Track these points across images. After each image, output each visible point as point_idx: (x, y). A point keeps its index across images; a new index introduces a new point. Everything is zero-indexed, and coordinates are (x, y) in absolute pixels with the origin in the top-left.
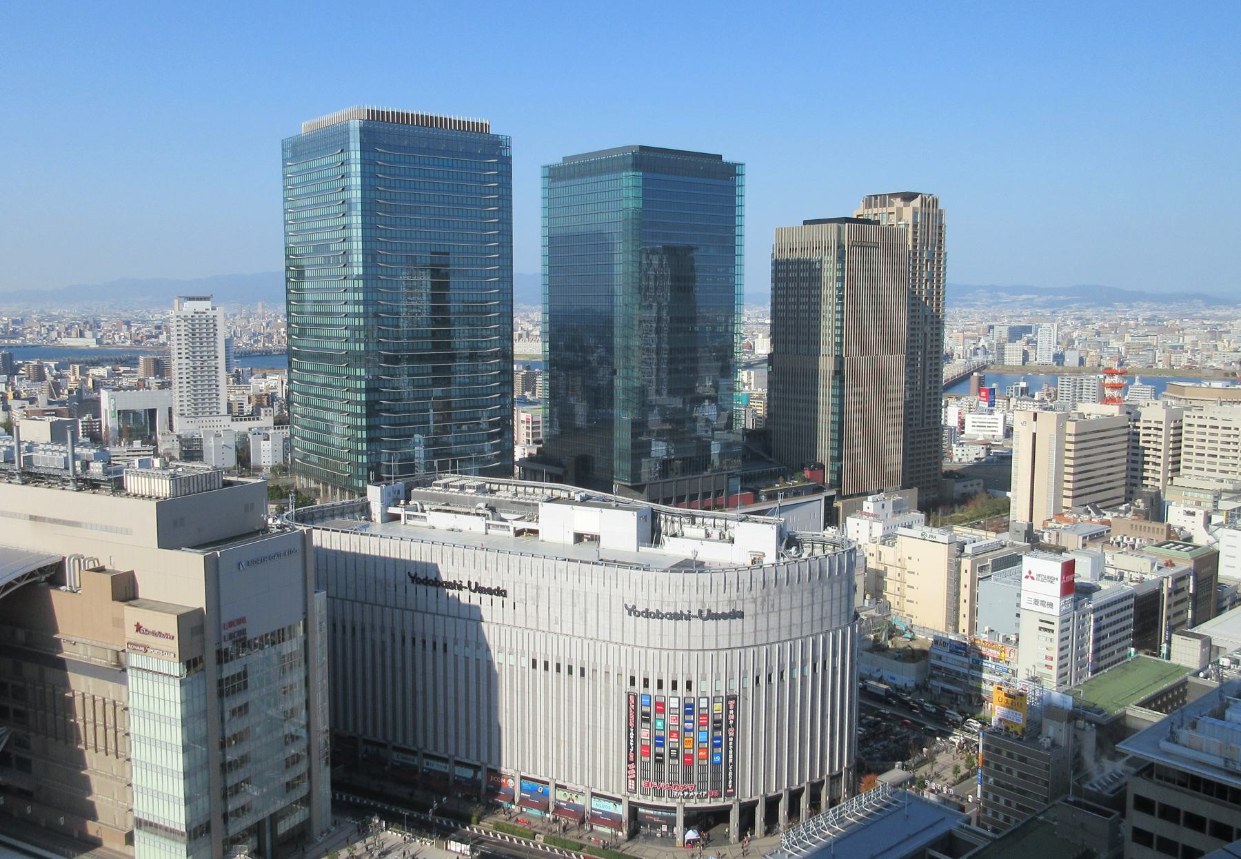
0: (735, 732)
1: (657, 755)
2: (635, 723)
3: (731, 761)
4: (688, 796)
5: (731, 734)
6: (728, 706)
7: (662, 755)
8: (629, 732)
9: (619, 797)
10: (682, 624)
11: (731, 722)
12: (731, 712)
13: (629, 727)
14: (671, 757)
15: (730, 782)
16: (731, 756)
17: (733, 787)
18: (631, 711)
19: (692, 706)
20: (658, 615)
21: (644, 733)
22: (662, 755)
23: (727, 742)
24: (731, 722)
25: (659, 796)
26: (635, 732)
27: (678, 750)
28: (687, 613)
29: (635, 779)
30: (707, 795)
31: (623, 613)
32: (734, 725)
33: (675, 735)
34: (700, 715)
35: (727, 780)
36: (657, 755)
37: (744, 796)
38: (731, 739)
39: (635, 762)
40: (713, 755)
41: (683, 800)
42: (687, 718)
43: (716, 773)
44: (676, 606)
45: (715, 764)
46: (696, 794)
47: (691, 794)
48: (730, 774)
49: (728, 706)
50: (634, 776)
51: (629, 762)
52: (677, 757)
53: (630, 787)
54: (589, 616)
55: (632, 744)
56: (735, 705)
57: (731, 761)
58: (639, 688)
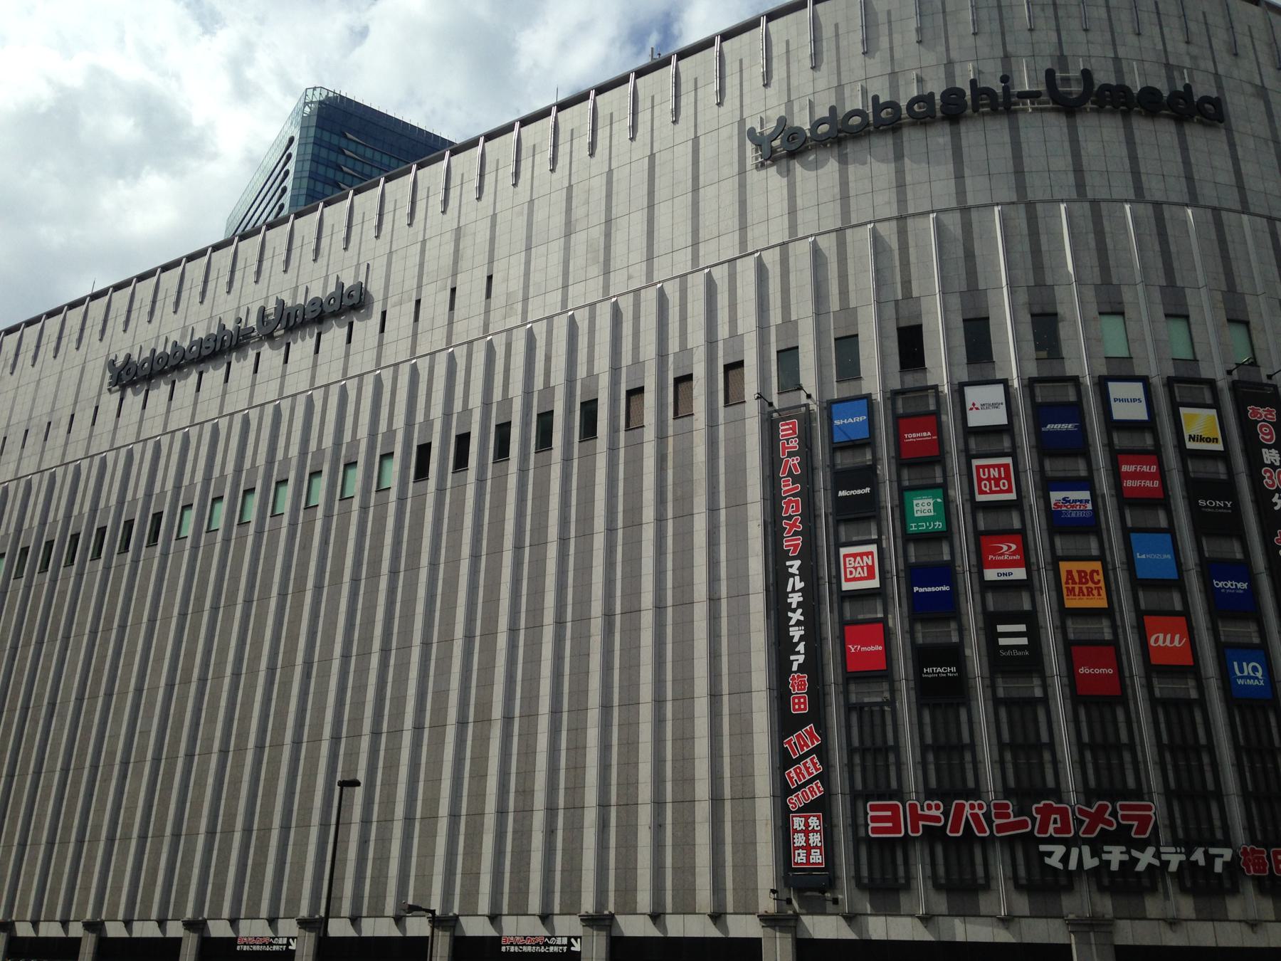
1: (923, 656)
2: (809, 534)
6: (1248, 430)
7: (954, 654)
14: (999, 662)
18: (787, 486)
19: (1075, 411)
26: (809, 573)
27: (1030, 618)
28: (998, 87)
31: (742, 172)
33: (1008, 549)
34: (1116, 456)
39: (817, 715)
40: (1225, 652)
41: (1106, 905)
42: (1055, 467)
46: (1174, 859)
47: (1146, 858)
49: (1248, 430)
50: (817, 790)
53: (800, 857)
54: (619, 237)
55: (796, 633)
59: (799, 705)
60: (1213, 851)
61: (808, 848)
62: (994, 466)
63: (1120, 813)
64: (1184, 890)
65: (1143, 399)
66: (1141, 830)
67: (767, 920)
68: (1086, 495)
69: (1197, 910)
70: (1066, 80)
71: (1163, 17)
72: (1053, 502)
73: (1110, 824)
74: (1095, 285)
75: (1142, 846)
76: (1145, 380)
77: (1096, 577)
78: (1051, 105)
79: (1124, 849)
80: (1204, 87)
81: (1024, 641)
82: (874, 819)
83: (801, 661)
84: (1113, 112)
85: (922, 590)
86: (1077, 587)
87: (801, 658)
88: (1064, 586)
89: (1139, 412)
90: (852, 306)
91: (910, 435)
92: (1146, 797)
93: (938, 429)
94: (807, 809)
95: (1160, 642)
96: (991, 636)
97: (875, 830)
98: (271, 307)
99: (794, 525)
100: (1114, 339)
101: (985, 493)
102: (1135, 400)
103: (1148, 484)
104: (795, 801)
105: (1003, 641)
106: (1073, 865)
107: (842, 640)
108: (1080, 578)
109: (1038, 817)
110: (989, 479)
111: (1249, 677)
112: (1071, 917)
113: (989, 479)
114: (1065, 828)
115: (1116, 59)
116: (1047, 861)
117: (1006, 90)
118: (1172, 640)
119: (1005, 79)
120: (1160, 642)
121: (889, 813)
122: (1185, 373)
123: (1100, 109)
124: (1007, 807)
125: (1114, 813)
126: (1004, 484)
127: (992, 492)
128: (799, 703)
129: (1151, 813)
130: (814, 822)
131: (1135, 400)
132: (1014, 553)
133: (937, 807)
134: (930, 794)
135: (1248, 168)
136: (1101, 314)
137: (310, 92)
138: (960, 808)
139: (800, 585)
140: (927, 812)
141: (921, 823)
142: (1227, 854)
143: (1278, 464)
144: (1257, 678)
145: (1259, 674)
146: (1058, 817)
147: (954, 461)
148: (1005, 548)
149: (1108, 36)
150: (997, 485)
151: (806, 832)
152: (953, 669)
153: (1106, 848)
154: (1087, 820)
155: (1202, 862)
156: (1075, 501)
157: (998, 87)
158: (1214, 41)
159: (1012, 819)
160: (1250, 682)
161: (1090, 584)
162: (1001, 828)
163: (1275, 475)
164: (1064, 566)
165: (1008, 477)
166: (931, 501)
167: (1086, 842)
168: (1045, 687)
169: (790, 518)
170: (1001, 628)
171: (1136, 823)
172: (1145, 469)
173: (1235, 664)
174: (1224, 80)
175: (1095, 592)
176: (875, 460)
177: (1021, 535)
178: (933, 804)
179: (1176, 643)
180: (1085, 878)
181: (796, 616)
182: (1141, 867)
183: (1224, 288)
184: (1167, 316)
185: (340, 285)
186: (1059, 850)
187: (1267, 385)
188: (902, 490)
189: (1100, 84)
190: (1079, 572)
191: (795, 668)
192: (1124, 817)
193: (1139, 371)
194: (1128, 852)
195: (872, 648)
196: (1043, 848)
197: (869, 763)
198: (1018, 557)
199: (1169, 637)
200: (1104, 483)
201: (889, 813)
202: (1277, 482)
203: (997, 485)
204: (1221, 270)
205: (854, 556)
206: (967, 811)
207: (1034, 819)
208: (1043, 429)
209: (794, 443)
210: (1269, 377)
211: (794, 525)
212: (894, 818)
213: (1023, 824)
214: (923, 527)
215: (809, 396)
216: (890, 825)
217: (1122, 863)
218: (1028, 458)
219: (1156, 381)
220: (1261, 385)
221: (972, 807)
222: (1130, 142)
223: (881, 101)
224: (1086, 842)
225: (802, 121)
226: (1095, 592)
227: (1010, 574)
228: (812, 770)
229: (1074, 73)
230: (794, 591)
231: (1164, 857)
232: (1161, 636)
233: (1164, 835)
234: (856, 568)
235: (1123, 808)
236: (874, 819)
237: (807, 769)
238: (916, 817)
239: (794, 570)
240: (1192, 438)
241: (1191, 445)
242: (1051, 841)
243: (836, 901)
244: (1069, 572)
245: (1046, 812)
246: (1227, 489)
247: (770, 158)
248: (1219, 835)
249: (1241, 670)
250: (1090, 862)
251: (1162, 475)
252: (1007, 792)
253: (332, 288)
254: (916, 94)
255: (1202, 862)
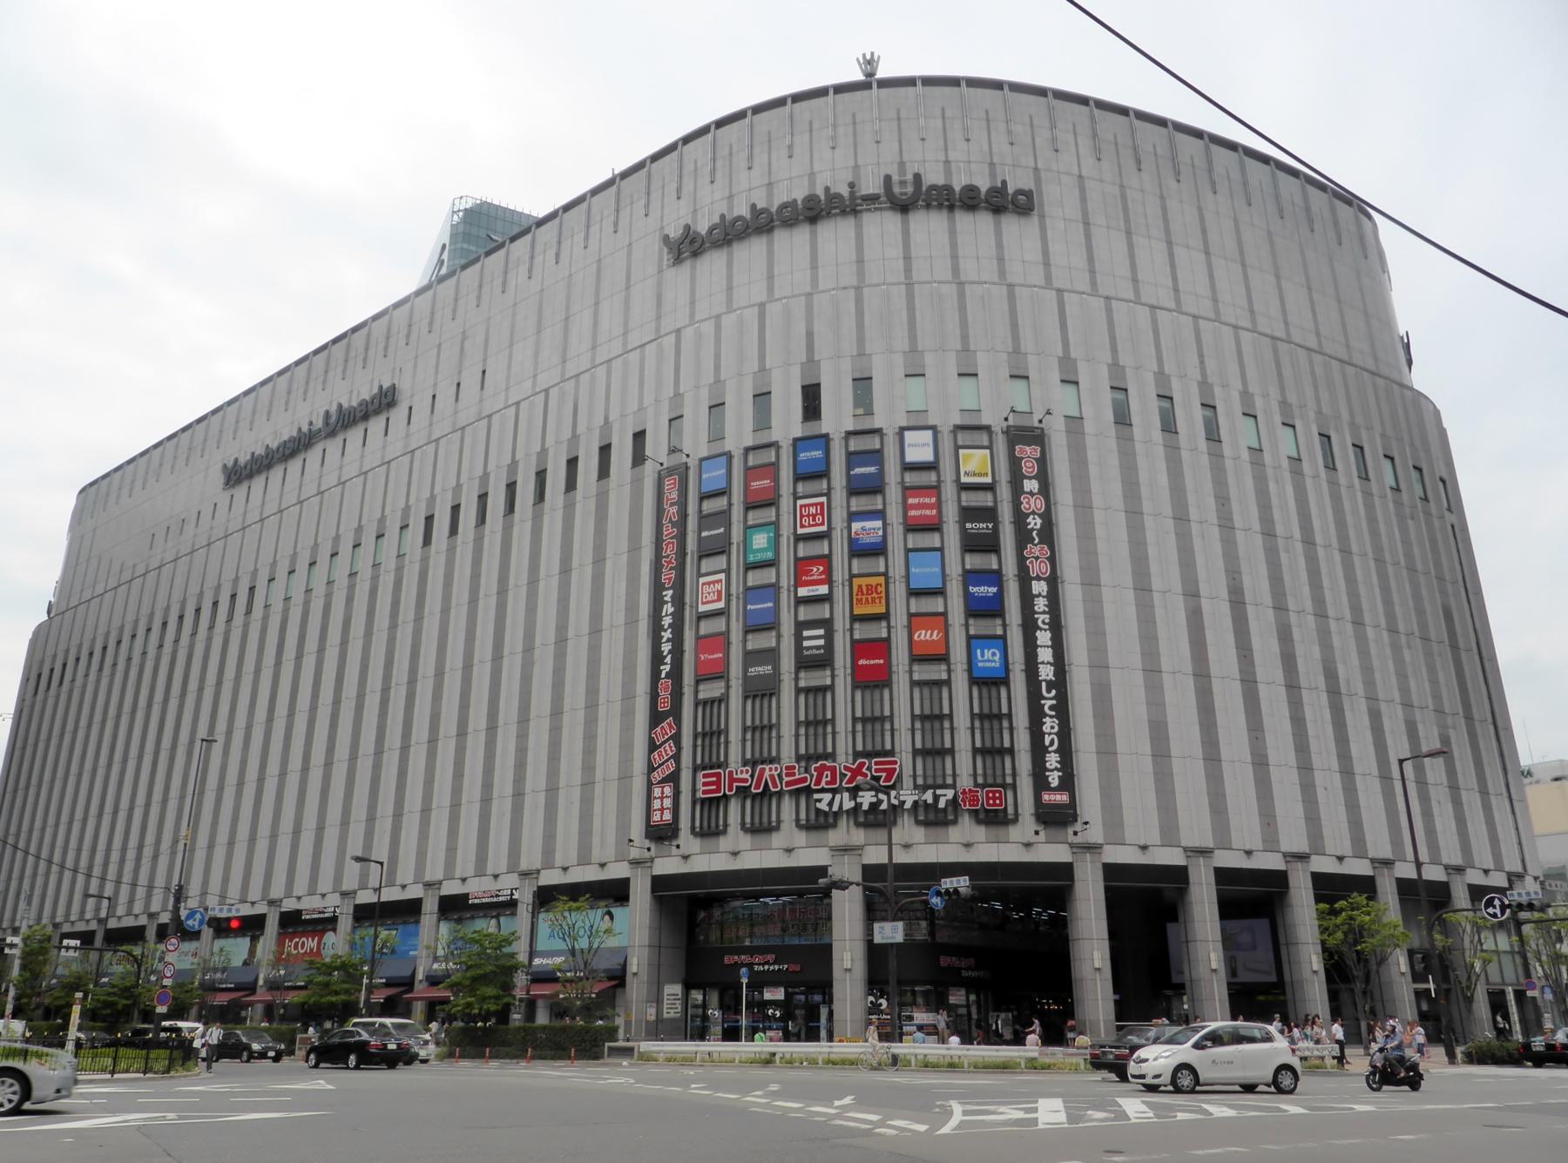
0: (1052, 560)
3: (1046, 672)
4: (874, 806)
5: (1038, 567)
7: (771, 655)
8: (657, 603)
9: (618, 871)
10: (835, 235)
11: (1035, 523)
12: (1031, 485)
13: (658, 588)
14: (806, 663)
15: (1052, 760)
16: (1045, 655)
17: (1068, 783)
19: (876, 456)
20: (761, 224)
21: (708, 590)
22: (771, 655)
23: (1027, 598)
24: (1035, 523)
25: (761, 829)
26: (679, 602)
27: (827, 624)
29: (674, 778)
30: (954, 802)
31: (660, 271)
32: (1048, 534)
34: (907, 490)
35: (1038, 751)
36: (750, 657)
37: (1116, 835)
38: (1039, 587)
39: (676, 712)
41: (858, 836)
42: (858, 504)
43: (990, 718)
44: (812, 183)
45: (989, 683)
46: (909, 797)
48: (1050, 725)
49: (1015, 463)
50: (672, 765)
51: (656, 718)
52: (823, 661)
53: (656, 817)
55: (666, 648)
56: (1043, 462)
57: (1046, 672)
58: (696, 445)
59: (664, 705)
60: (939, 792)
61: (662, 810)
62: (812, 505)
63: (874, 767)
64: (918, 823)
65: (906, 446)
66: (888, 779)
67: (636, 863)
68: (879, 524)
69: (926, 836)
70: (903, 183)
71: (991, 123)
72: (853, 531)
73: (866, 775)
74: (904, 352)
75: (886, 790)
76: (933, 428)
77: (879, 589)
78: (888, 205)
79: (873, 793)
80: (1017, 181)
81: (821, 642)
82: (705, 784)
83: (668, 670)
84: (940, 206)
85: (753, 607)
86: (864, 597)
87: (668, 668)
88: (855, 597)
89: (927, 455)
90: (722, 379)
91: (755, 484)
92: (898, 755)
93: (776, 479)
94: (664, 781)
95: (922, 637)
96: (799, 639)
97: (705, 792)
98: (334, 409)
99: (670, 562)
100: (915, 395)
101: (805, 526)
102: (924, 445)
103: (928, 512)
104: (657, 776)
105: (806, 644)
106: (835, 808)
107: (698, 650)
108: (868, 589)
109: (815, 774)
110: (808, 516)
111: (989, 661)
112: (832, 844)
113: (808, 516)
114: (833, 781)
115: (947, 162)
116: (818, 805)
117: (852, 194)
118: (931, 635)
119: (852, 185)
120: (922, 637)
121: (714, 779)
122: (968, 422)
123: (928, 206)
124: (794, 767)
125: (869, 769)
126: (819, 519)
127: (810, 526)
128: (664, 703)
129: (897, 766)
130: (668, 790)
131: (924, 445)
132: (821, 574)
133: (747, 772)
134: (745, 764)
135: (1052, 248)
136: (906, 376)
137: (457, 202)
138: (763, 771)
139: (671, 610)
140: (739, 776)
141: (735, 784)
142: (950, 793)
143: (1036, 491)
144: (995, 661)
145: (997, 658)
146: (829, 773)
147: (786, 502)
148: (815, 570)
149: (941, 143)
150: (814, 520)
151: (662, 798)
152: (770, 667)
153: (860, 794)
154: (849, 774)
155: (930, 801)
156: (870, 529)
157: (844, 191)
158: (1037, 140)
159: (797, 777)
160: (988, 665)
161: (875, 595)
162: (788, 784)
163: (1032, 500)
164: (856, 582)
165: (822, 514)
166: (766, 535)
167: (848, 790)
168: (833, 677)
169: (667, 557)
170: (806, 633)
171: (884, 775)
172: (927, 500)
173: (979, 651)
174: (1043, 175)
175: (877, 601)
176: (730, 505)
177: (826, 560)
178: (744, 769)
179: (934, 637)
180: (845, 816)
181: (667, 635)
182: (884, 806)
183: (1011, 350)
184: (959, 375)
185: (381, 387)
186: (827, 797)
187: (1037, 428)
188: (747, 528)
189: (929, 183)
190: (867, 586)
191: (663, 676)
192: (877, 771)
193: (931, 423)
194: (876, 796)
195: (715, 656)
196: (816, 796)
197: (707, 742)
198: (823, 576)
199: (929, 632)
200: (894, 514)
201: (714, 779)
202: (1033, 506)
203: (814, 520)
204: (1009, 335)
205: (709, 583)
206: (767, 773)
207: (812, 776)
208: (852, 473)
209: (674, 495)
210: (1040, 421)
211: (670, 562)
212: (718, 783)
213: (804, 780)
214: (759, 557)
215: (688, 456)
216: (714, 787)
217: (872, 804)
218: (839, 495)
219: (945, 430)
220: (1033, 429)
221: (771, 769)
222: (952, 232)
223: (758, 207)
224: (848, 790)
225: (702, 228)
226: (877, 601)
227: (817, 590)
228: (669, 752)
229: (909, 177)
230: (666, 615)
231: (902, 798)
232: (924, 632)
233: (907, 782)
234: (709, 593)
235: (876, 763)
236: (705, 784)
237: (666, 751)
238: (732, 780)
239: (667, 599)
240: (967, 474)
241: (964, 479)
242: (823, 791)
243: (678, 847)
244: (860, 586)
245: (820, 771)
246: (990, 514)
247: (678, 260)
248: (949, 781)
249: (983, 655)
250: (848, 804)
251: (939, 505)
252: (799, 758)
253: (376, 390)
254: (785, 200)
255: (930, 801)
